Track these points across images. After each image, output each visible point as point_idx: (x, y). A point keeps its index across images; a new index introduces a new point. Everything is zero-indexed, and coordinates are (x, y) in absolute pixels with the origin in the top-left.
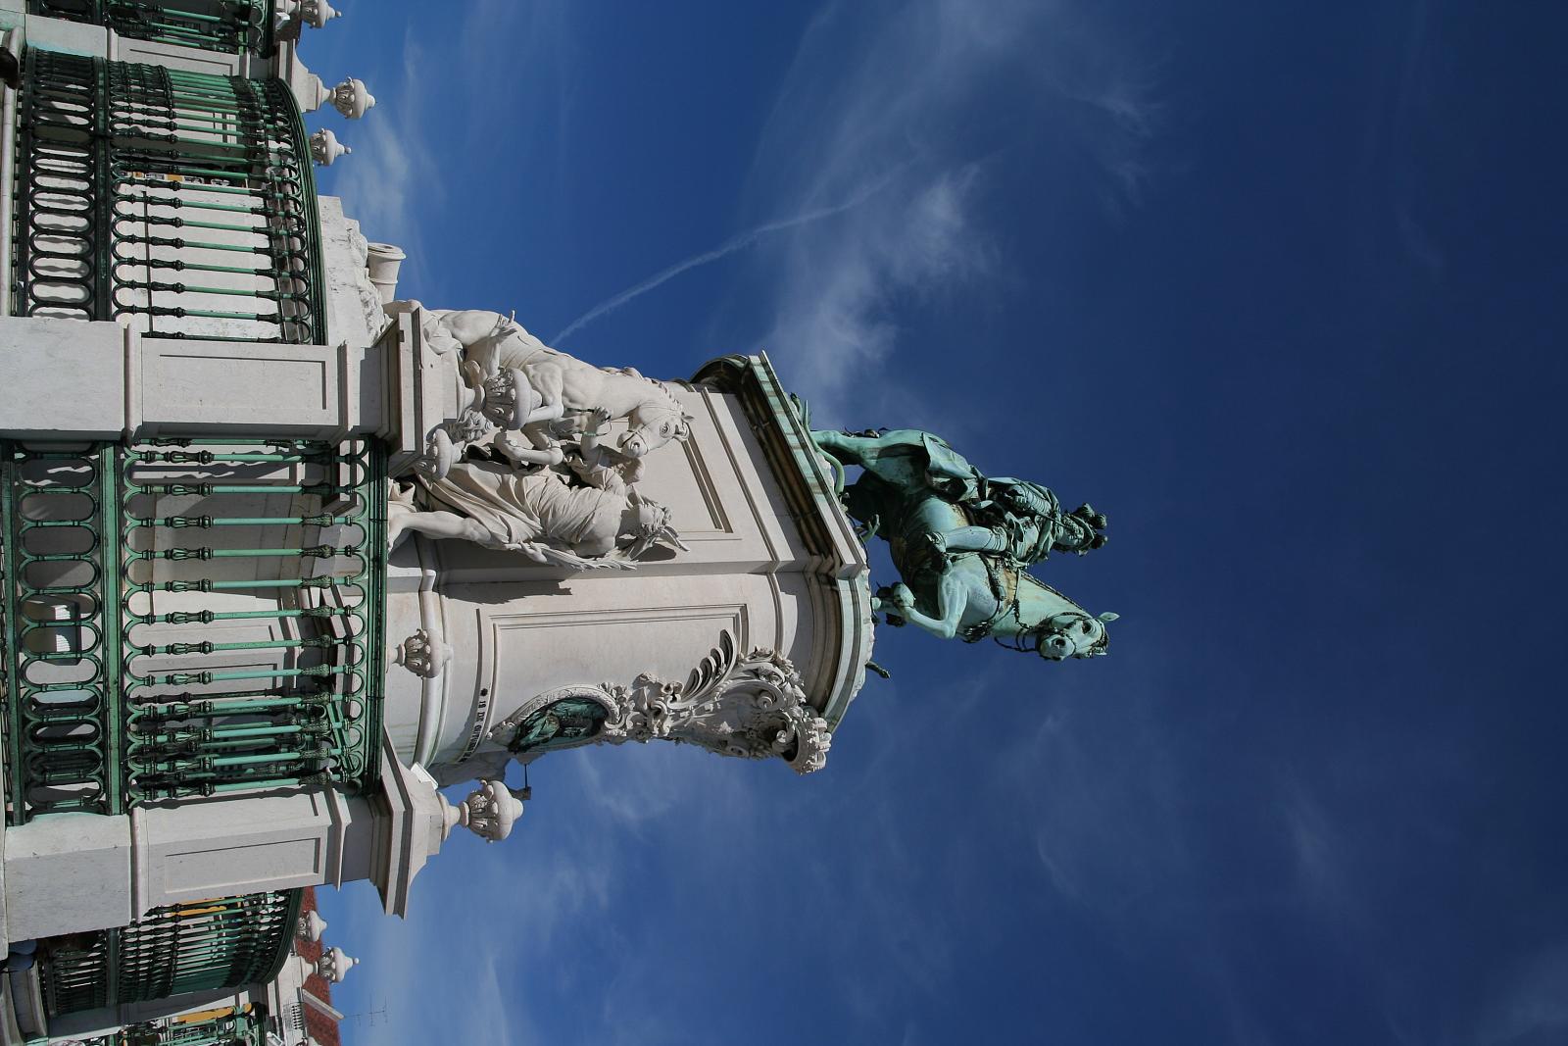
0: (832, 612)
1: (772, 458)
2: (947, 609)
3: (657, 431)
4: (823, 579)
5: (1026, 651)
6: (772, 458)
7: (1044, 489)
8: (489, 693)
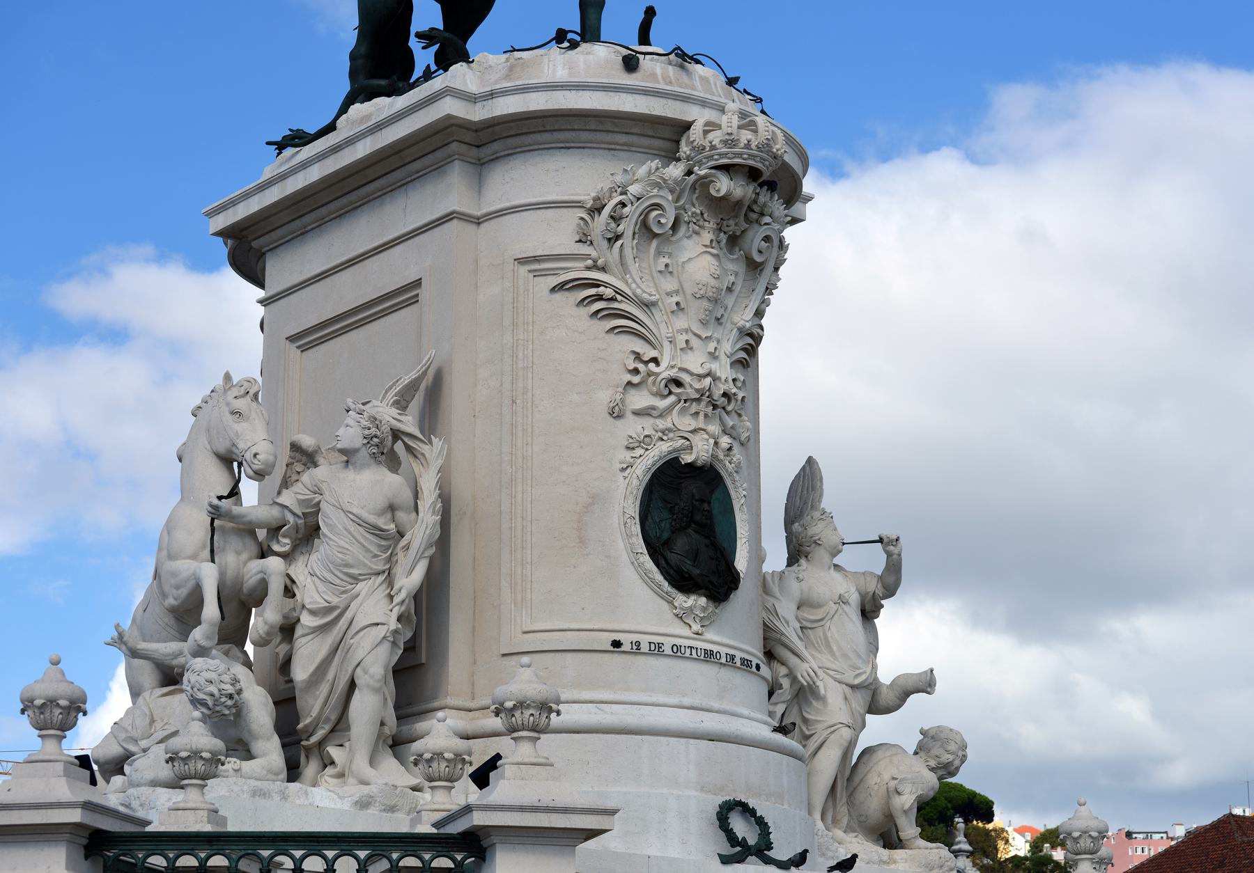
3: (240, 427)
8: (617, 637)
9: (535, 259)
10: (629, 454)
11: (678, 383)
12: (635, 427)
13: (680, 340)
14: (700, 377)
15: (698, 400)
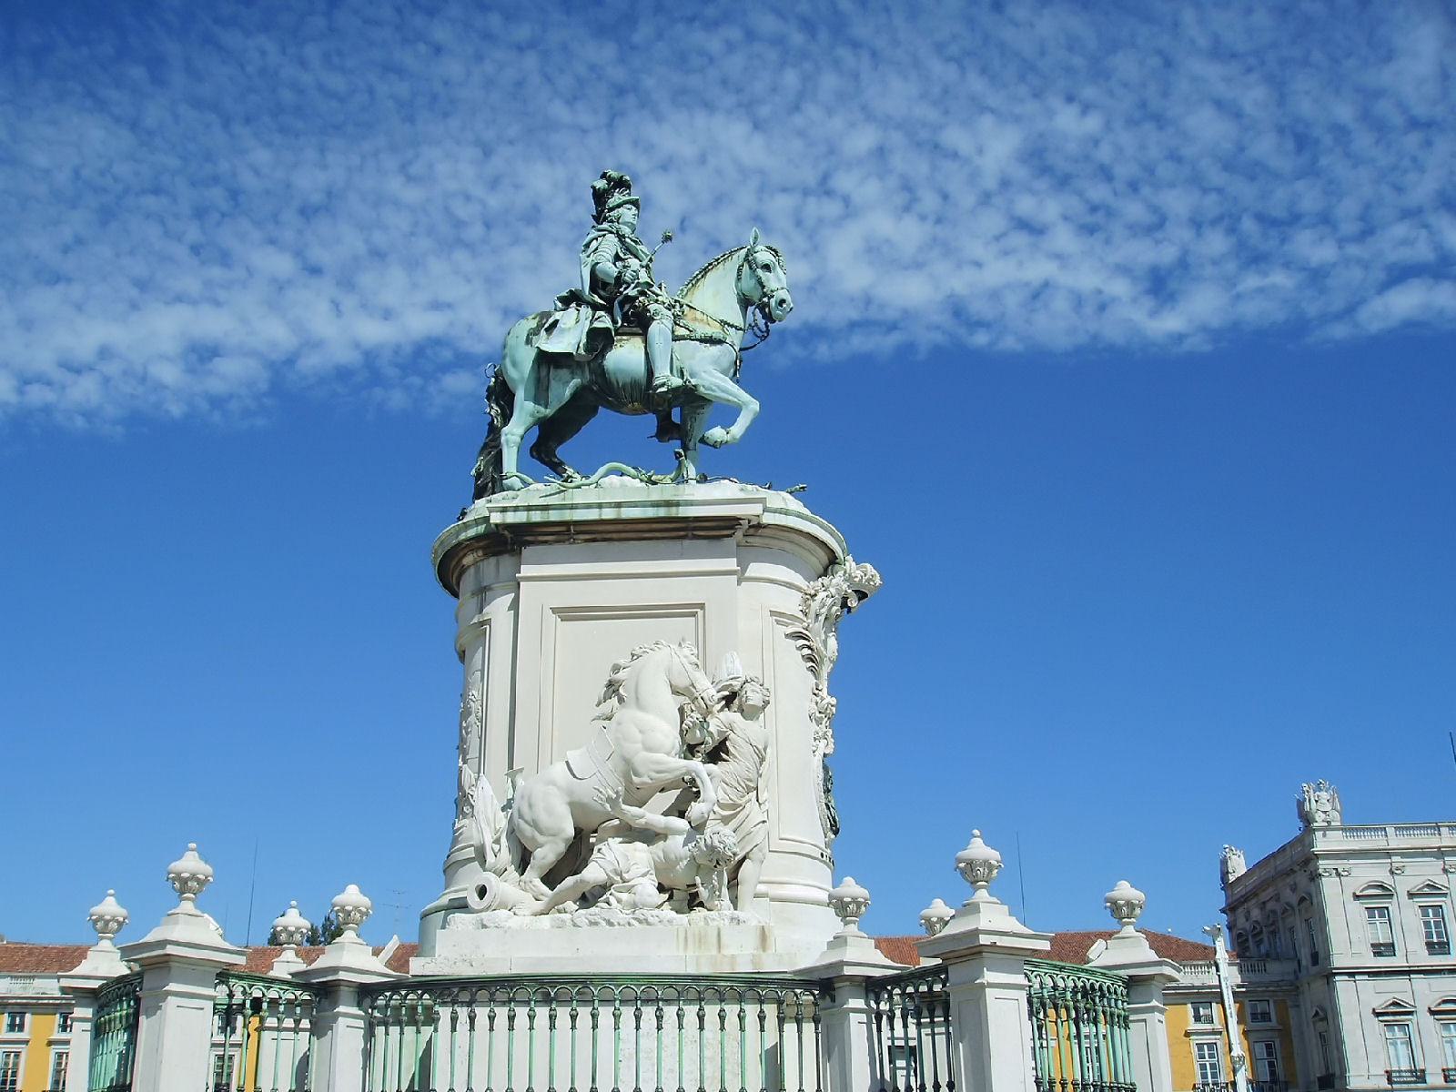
0: (782, 533)
1: (614, 536)
2: (730, 398)
4: (752, 531)
5: (768, 331)
6: (614, 536)
7: (594, 234)
9: (781, 614)
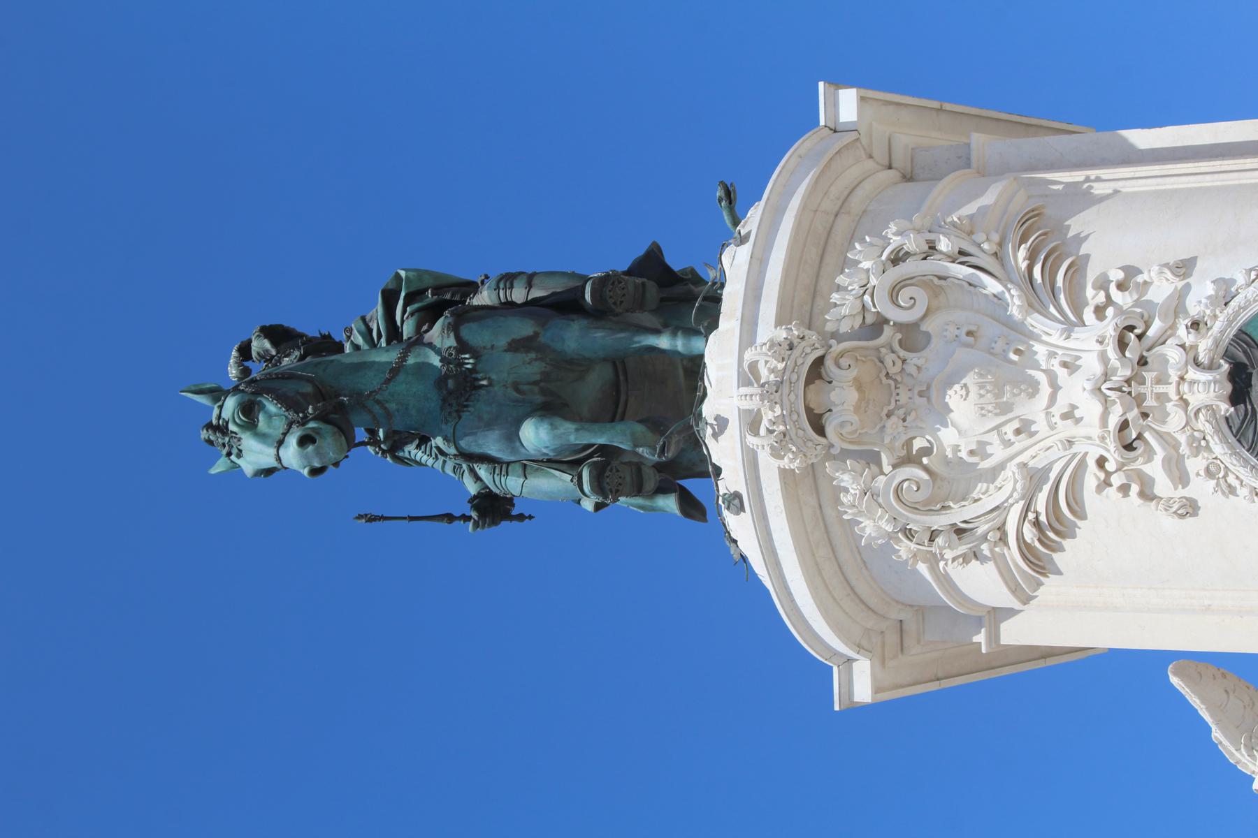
10: (1243, 492)
11: (1124, 425)
12: (1201, 488)
13: (1067, 429)
14: (1106, 401)
15: (1140, 399)
